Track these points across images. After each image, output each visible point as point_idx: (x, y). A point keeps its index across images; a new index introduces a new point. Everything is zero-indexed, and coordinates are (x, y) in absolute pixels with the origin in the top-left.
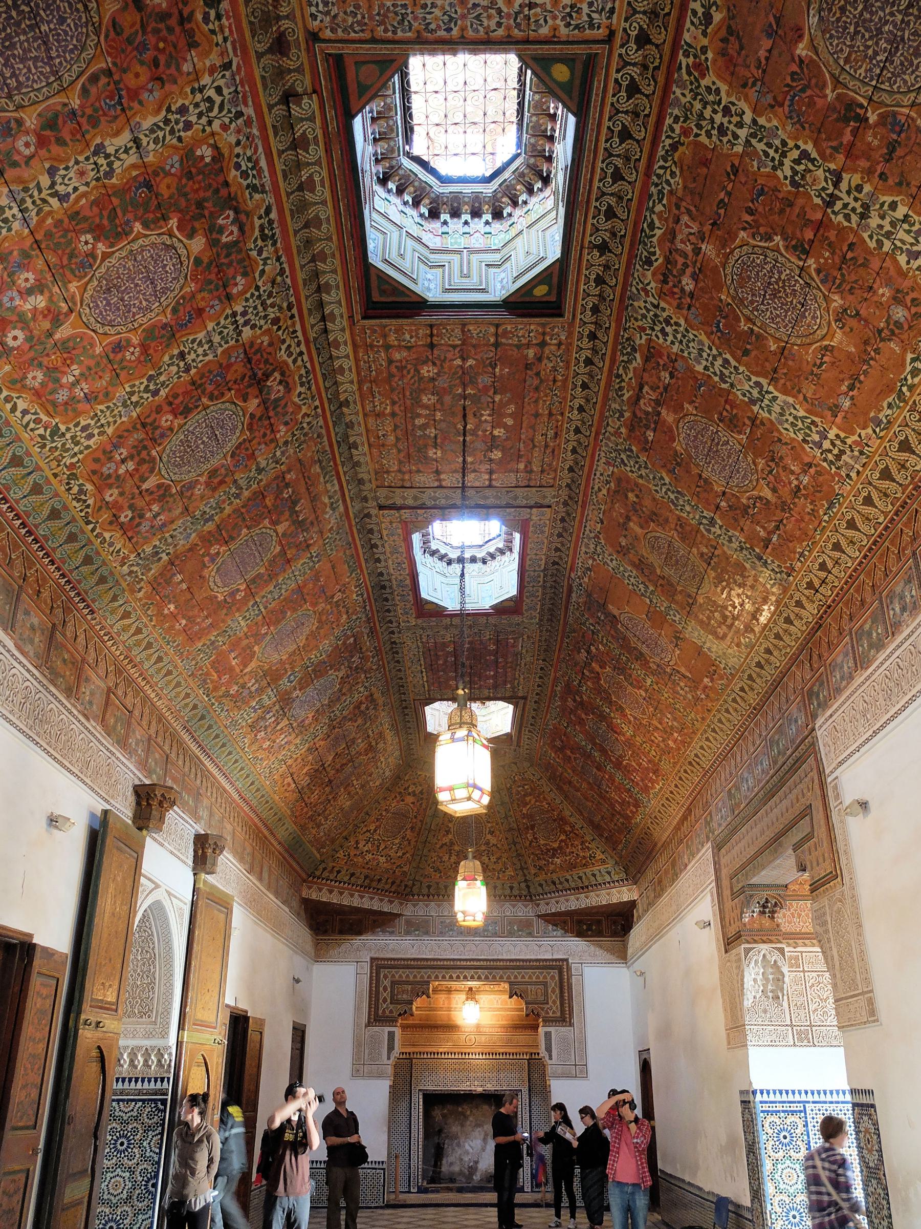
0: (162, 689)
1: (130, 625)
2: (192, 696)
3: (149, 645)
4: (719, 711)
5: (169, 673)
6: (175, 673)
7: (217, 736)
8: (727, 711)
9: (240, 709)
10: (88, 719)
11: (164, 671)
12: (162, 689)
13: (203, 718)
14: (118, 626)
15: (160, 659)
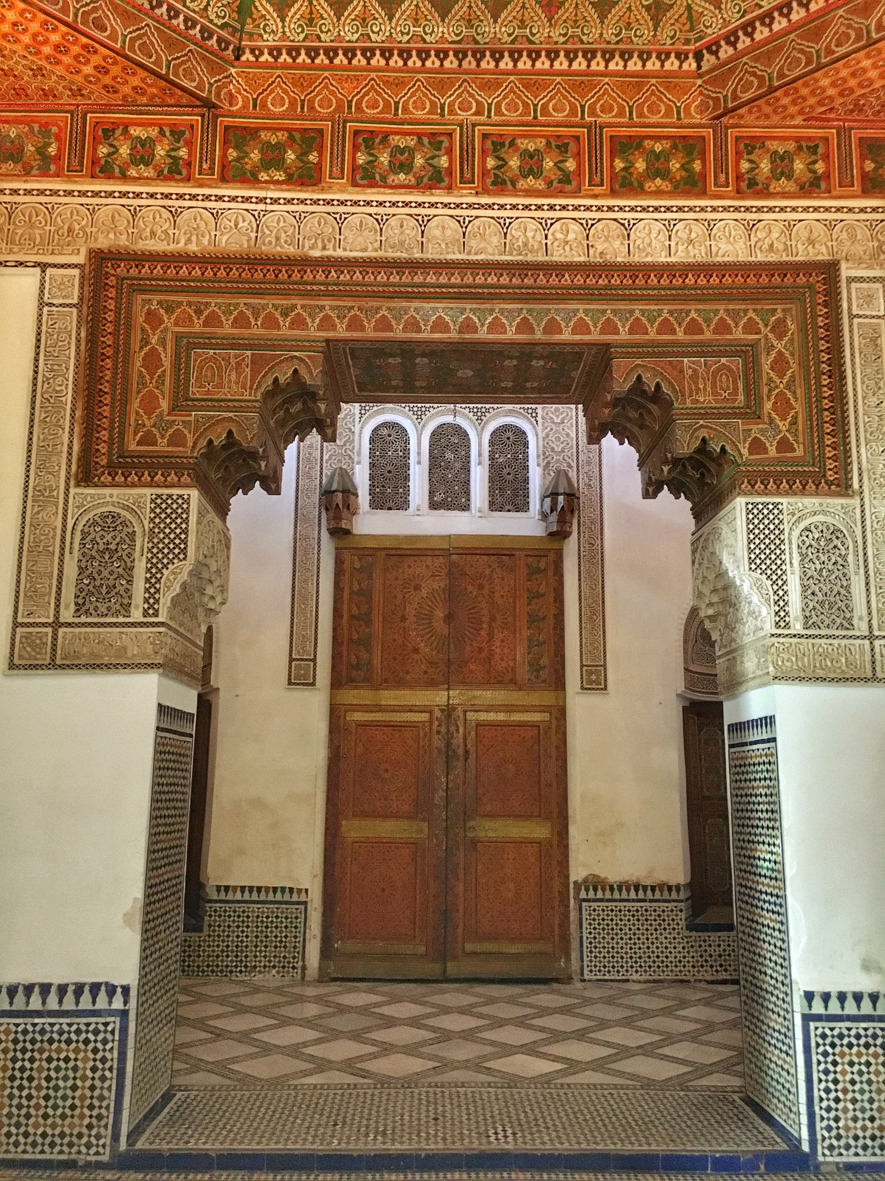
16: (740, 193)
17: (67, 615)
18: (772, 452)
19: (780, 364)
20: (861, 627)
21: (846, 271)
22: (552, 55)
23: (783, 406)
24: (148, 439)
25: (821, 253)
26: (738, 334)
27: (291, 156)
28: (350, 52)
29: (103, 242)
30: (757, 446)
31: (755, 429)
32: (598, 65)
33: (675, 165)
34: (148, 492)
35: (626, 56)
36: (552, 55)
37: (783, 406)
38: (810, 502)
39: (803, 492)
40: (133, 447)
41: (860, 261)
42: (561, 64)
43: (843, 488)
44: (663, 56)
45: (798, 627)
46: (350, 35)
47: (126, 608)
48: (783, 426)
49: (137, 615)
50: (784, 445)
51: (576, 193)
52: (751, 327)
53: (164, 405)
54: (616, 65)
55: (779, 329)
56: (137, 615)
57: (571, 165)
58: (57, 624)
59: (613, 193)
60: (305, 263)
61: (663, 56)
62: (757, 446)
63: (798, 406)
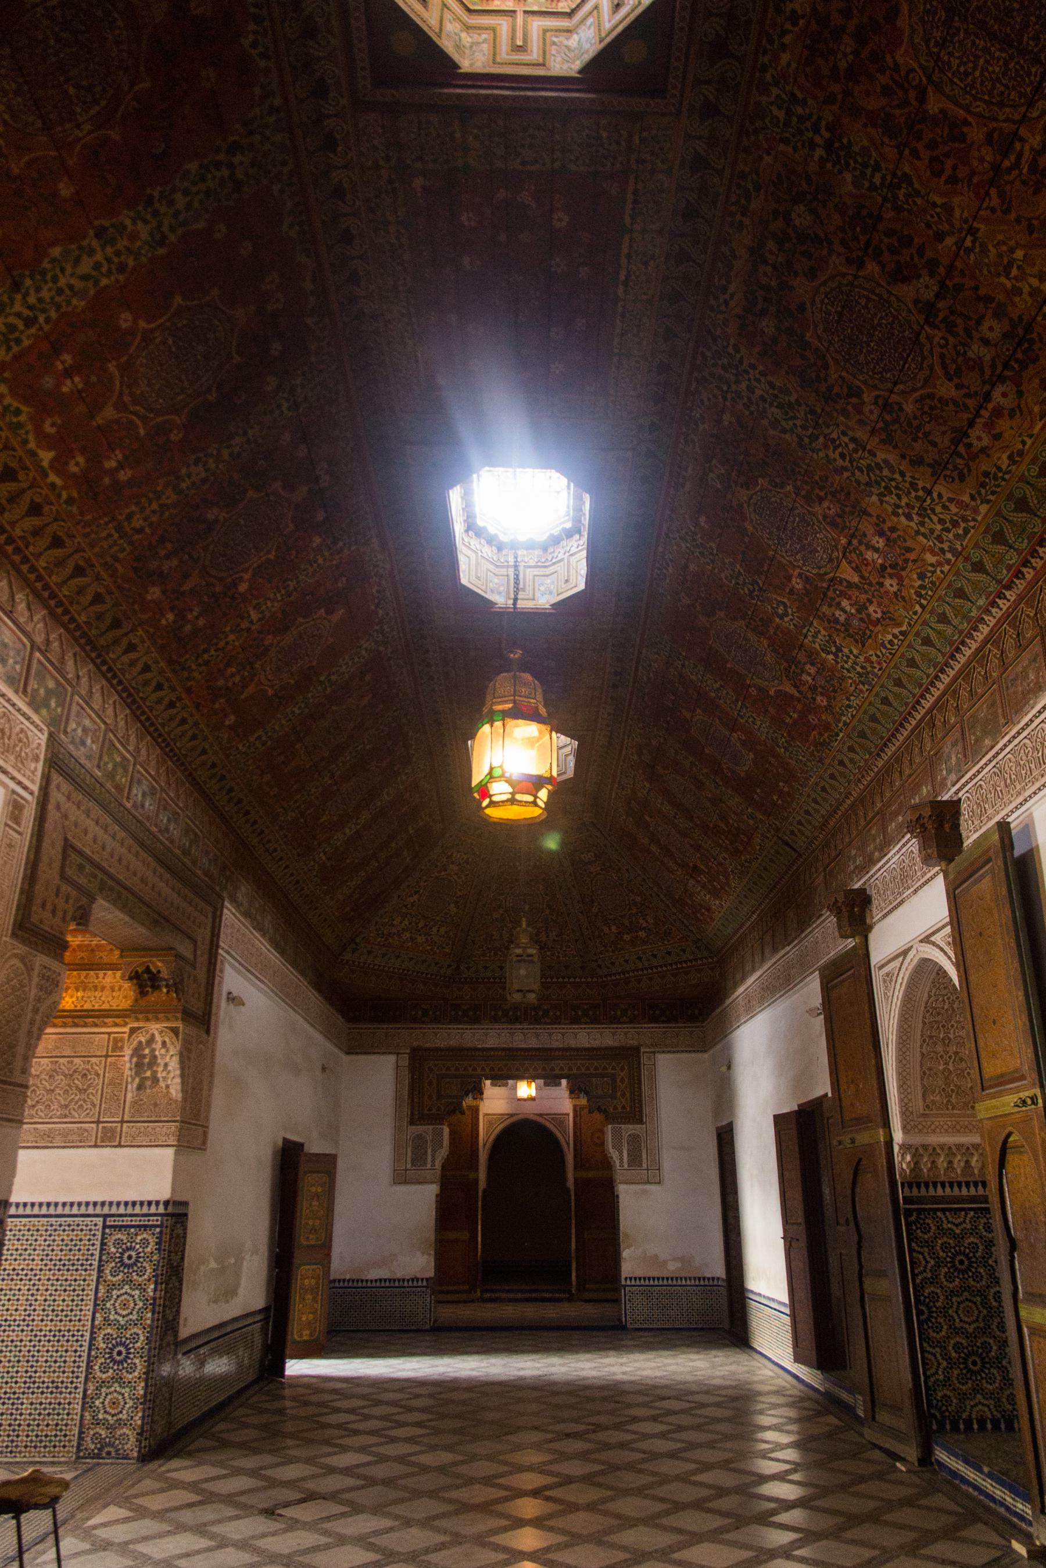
0: (840, 794)
1: (799, 830)
2: (840, 757)
3: (807, 812)
4: (196, 724)
5: (823, 789)
6: (823, 783)
7: (885, 701)
8: (194, 737)
9: (843, 678)
10: (821, 915)
11: (824, 794)
12: (840, 794)
13: (862, 735)
14: (810, 828)
15: (815, 801)
16: (611, 1023)
17: (409, 1166)
18: (620, 1109)
19: (622, 1081)
20: (645, 1166)
21: (642, 1050)
22: (552, 978)
23: (623, 1095)
24: (430, 1109)
25: (635, 1043)
26: (610, 1071)
27: (471, 1013)
28: (489, 978)
29: (415, 1044)
30: (615, 1108)
31: (615, 1102)
32: (566, 980)
33: (591, 1013)
34: (431, 1127)
35: (575, 978)
36: (552, 978)
37: (623, 1095)
38: (631, 1126)
39: (628, 1123)
40: (426, 1112)
41: (647, 1046)
42: (555, 980)
43: (640, 1121)
44: (586, 978)
45: (626, 1166)
46: (489, 974)
47: (425, 1164)
48: (623, 1101)
49: (429, 1166)
50: (623, 1107)
51: (559, 1023)
52: (614, 1068)
53: (435, 1098)
54: (572, 980)
55: (623, 1069)
56: (429, 1166)
57: (558, 1013)
58: (406, 1170)
59: (572, 1023)
60: (476, 1049)
61: (586, 978)
62: (615, 1108)
63: (628, 1094)
